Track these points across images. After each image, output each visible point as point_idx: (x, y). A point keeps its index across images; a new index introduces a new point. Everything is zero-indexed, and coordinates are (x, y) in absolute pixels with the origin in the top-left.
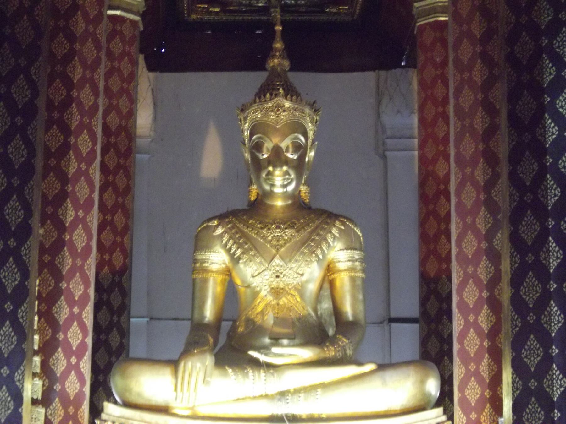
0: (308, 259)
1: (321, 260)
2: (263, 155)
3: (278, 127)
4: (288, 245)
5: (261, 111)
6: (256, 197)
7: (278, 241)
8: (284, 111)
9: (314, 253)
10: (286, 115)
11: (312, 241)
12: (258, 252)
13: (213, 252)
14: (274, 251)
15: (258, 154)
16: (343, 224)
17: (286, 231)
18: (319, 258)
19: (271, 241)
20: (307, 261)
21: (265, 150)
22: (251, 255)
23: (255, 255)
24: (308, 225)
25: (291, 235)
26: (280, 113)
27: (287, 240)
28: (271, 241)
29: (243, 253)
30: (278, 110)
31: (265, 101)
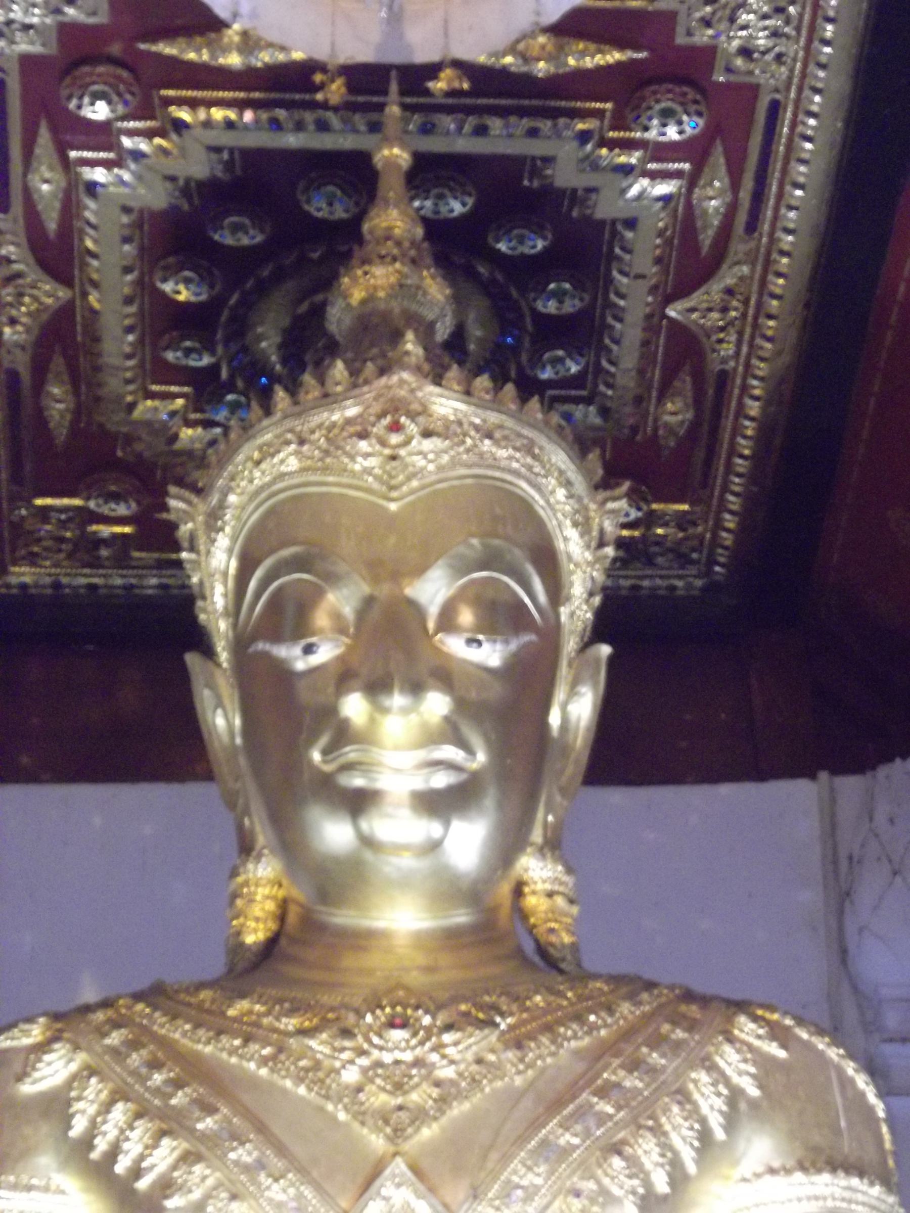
0: (591, 1185)
1: (665, 1197)
2: (309, 650)
3: (393, 507)
4: (458, 1109)
5: (302, 442)
6: (273, 926)
7: (399, 1087)
8: (427, 434)
9: (619, 1153)
10: (438, 453)
11: (603, 1092)
12: (281, 1150)
13: (15, 1187)
14: (377, 1142)
15: (282, 651)
16: (777, 1033)
17: (447, 1038)
18: (647, 1183)
19: (359, 1089)
20: (577, 1194)
21: (321, 619)
22: (236, 1163)
23: (260, 1165)
24: (579, 1018)
25: (479, 1061)
26: (407, 443)
27: (452, 1082)
28: (359, 1089)
29: (188, 1158)
30: (396, 427)
31: (326, 395)
